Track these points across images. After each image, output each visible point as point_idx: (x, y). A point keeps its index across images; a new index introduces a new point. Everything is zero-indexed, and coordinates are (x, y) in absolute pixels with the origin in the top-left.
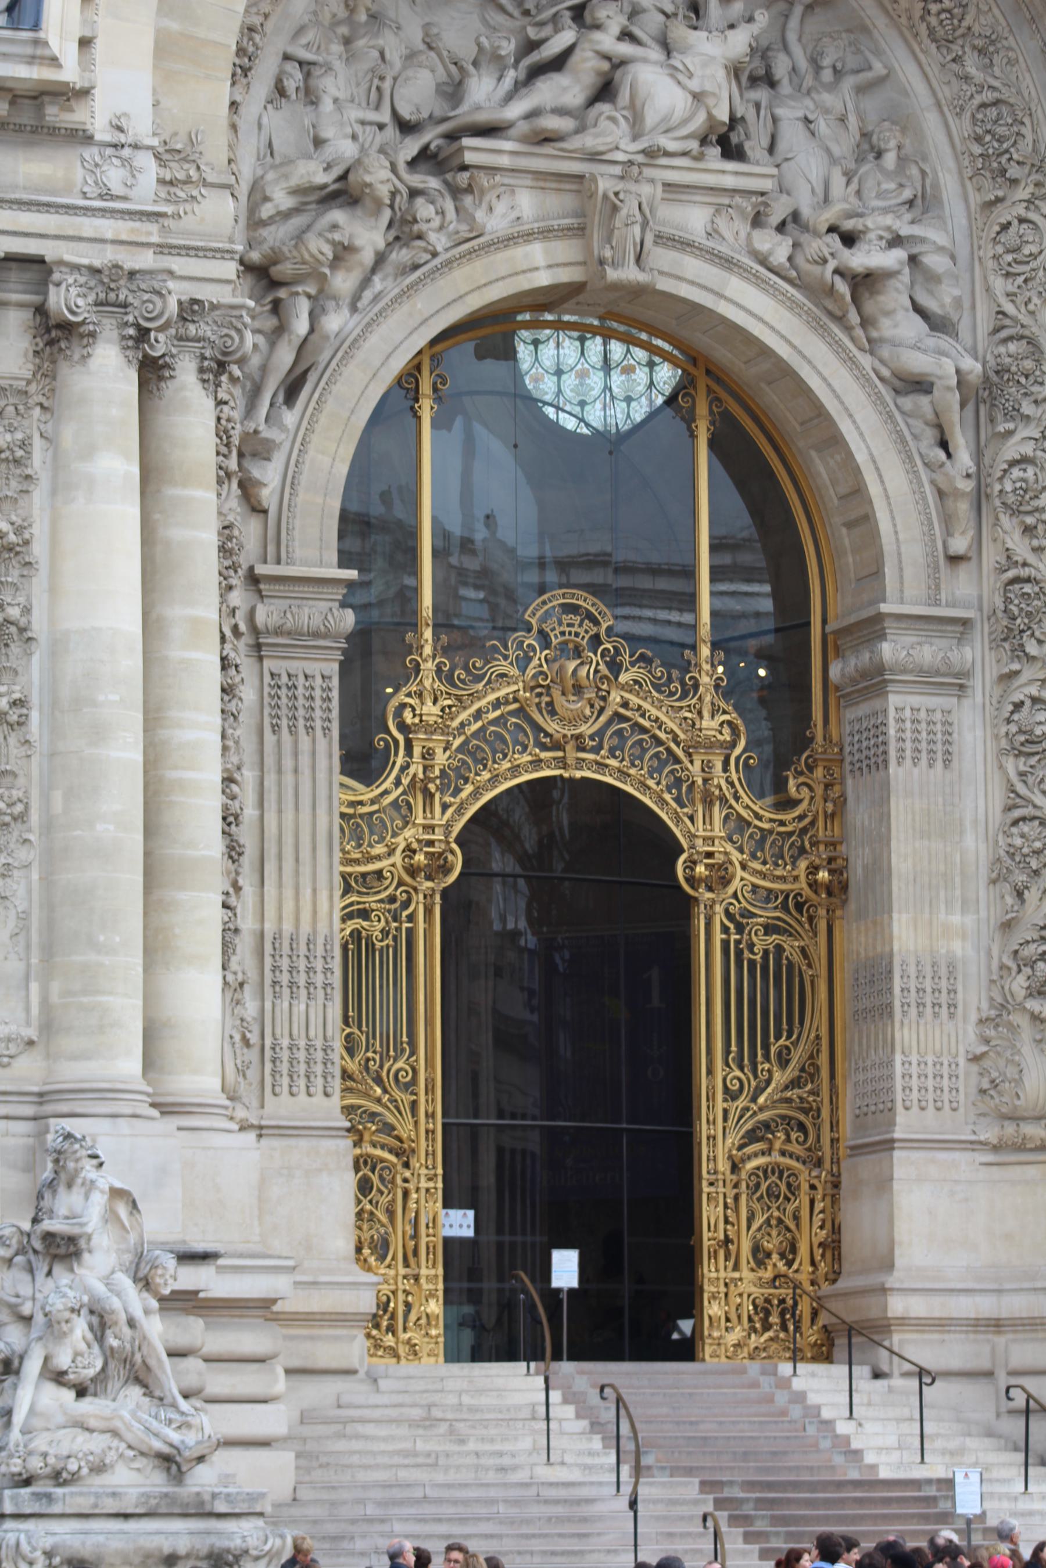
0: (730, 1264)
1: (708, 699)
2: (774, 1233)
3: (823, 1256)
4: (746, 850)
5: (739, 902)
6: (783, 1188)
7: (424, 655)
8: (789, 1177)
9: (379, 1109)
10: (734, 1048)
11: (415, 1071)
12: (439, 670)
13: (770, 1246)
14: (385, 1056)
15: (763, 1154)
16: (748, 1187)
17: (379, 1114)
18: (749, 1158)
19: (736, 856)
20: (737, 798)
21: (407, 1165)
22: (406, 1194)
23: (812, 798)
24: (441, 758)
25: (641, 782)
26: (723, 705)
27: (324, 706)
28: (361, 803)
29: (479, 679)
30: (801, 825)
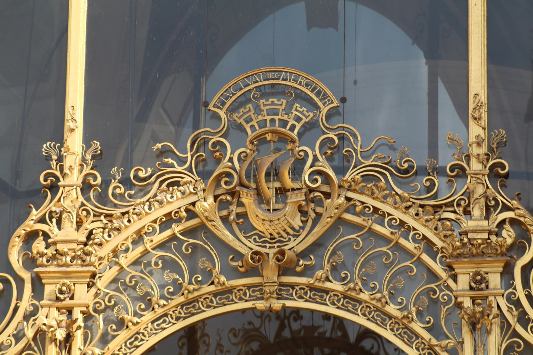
1: (480, 190)
12: (86, 187)
20: (523, 319)
25: (377, 309)
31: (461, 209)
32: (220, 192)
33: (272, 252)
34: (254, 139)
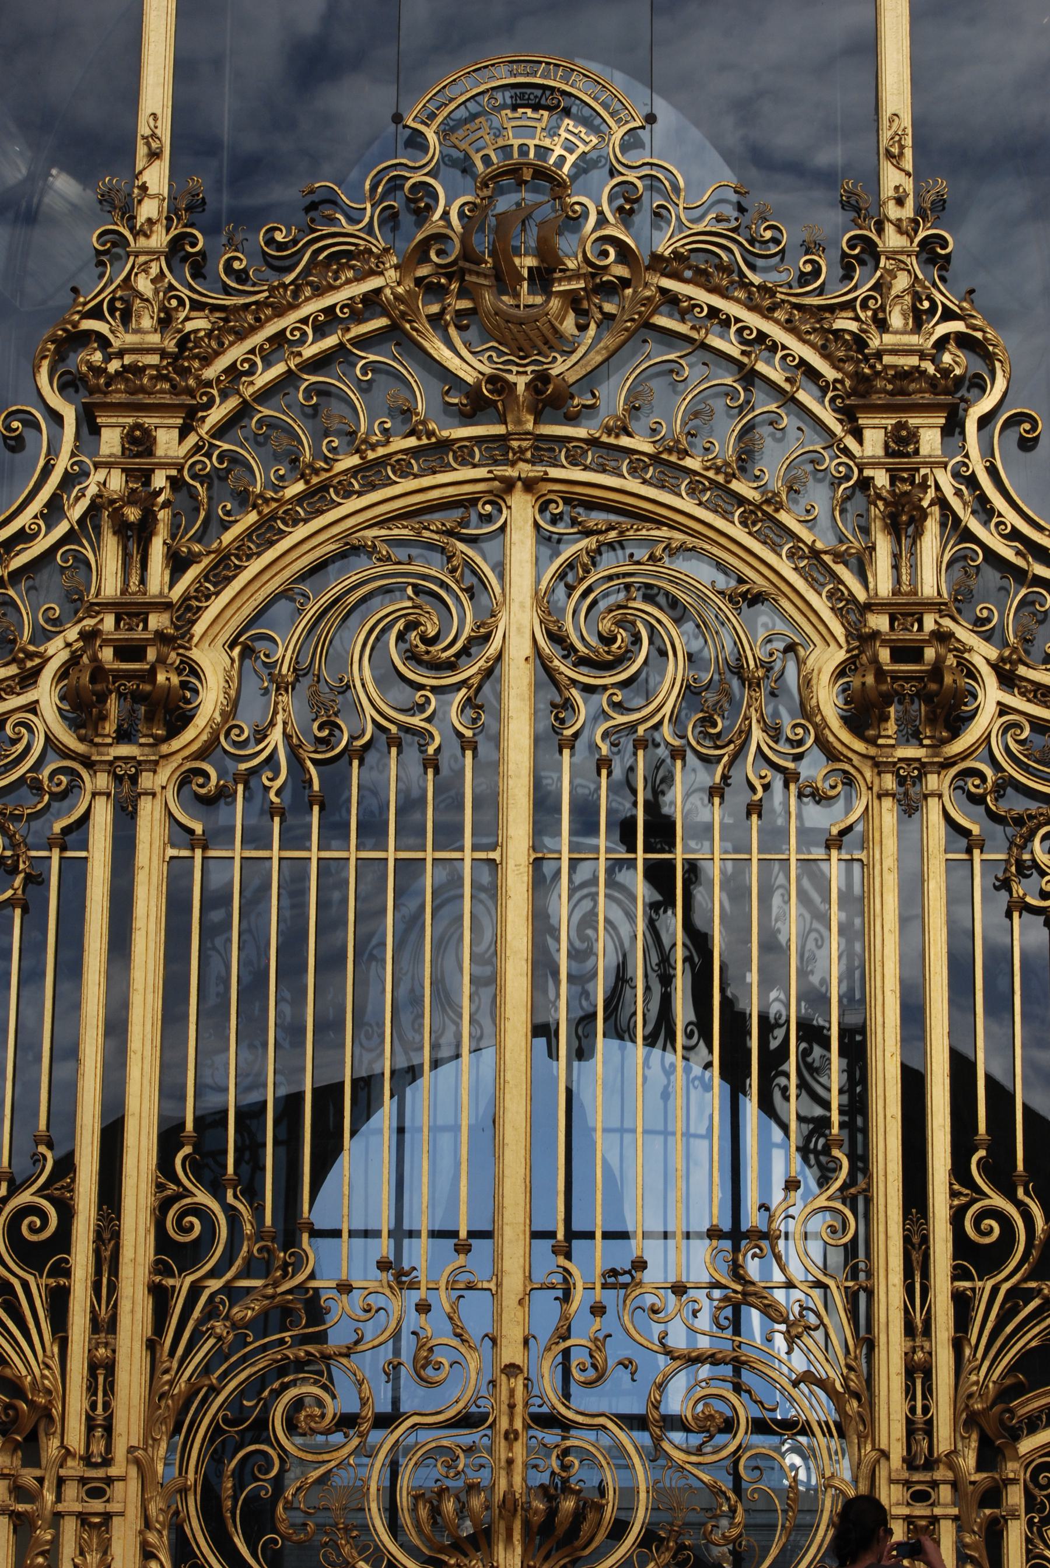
1: (901, 282)
7: (141, 219)
11: (67, 1212)
16: (1029, 1496)
20: (985, 510)
31: (870, 313)
32: (423, 271)
33: (521, 383)
34: (491, 179)
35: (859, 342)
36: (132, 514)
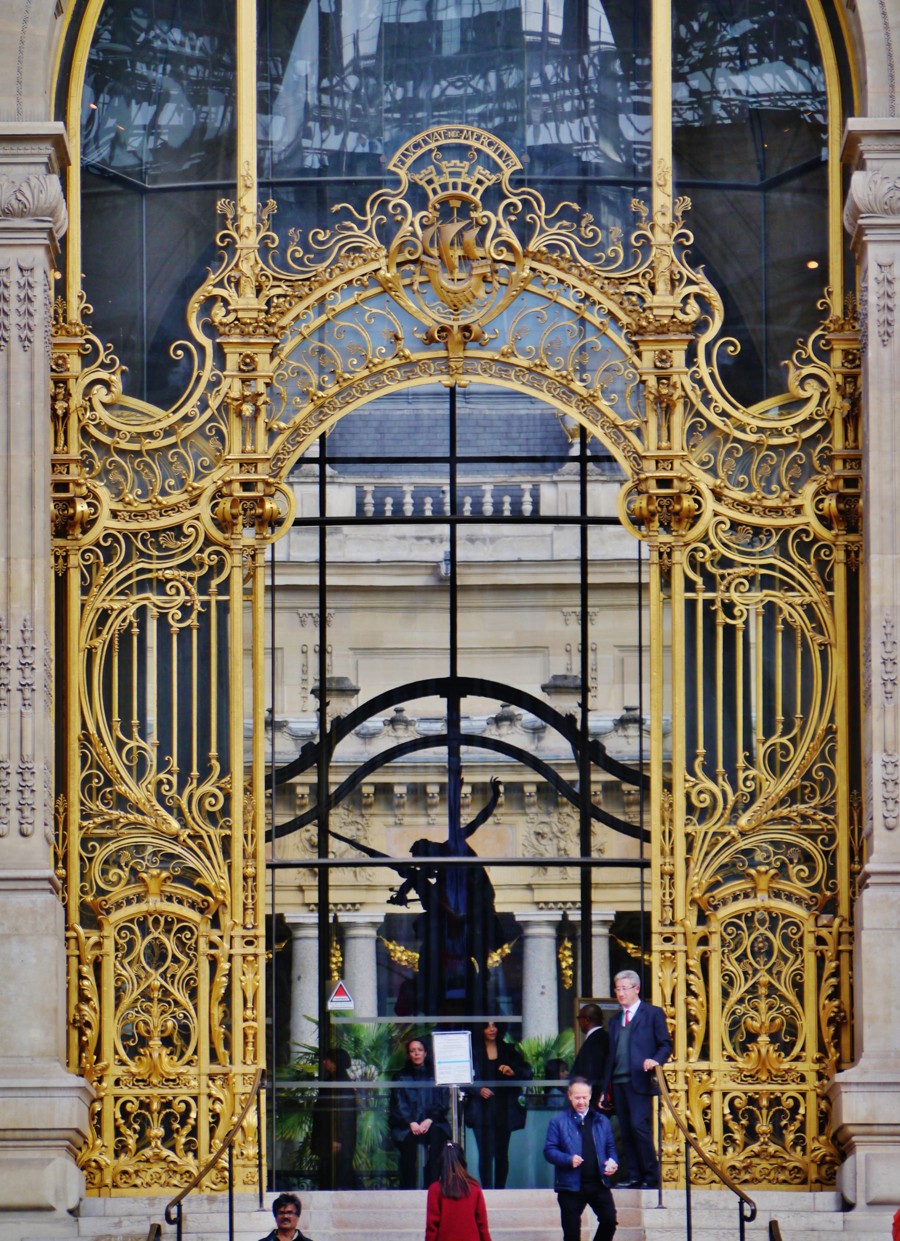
0: (695, 1051)
1: (665, 262)
2: (763, 1005)
3: (837, 1036)
4: (721, 474)
5: (712, 547)
6: (777, 943)
7: (243, 229)
8: (785, 926)
9: (178, 850)
10: (701, 750)
11: (228, 797)
12: (264, 249)
13: (757, 1025)
14: (183, 779)
15: (746, 896)
16: (723, 940)
17: (172, 856)
18: (724, 902)
19: (705, 482)
20: (707, 400)
21: (215, 923)
22: (214, 963)
23: (823, 395)
24: (265, 366)
26: (687, 272)
27: (22, 310)
28: (150, 435)
29: (321, 256)
30: (806, 434)
35: (641, 298)
36: (247, 409)
